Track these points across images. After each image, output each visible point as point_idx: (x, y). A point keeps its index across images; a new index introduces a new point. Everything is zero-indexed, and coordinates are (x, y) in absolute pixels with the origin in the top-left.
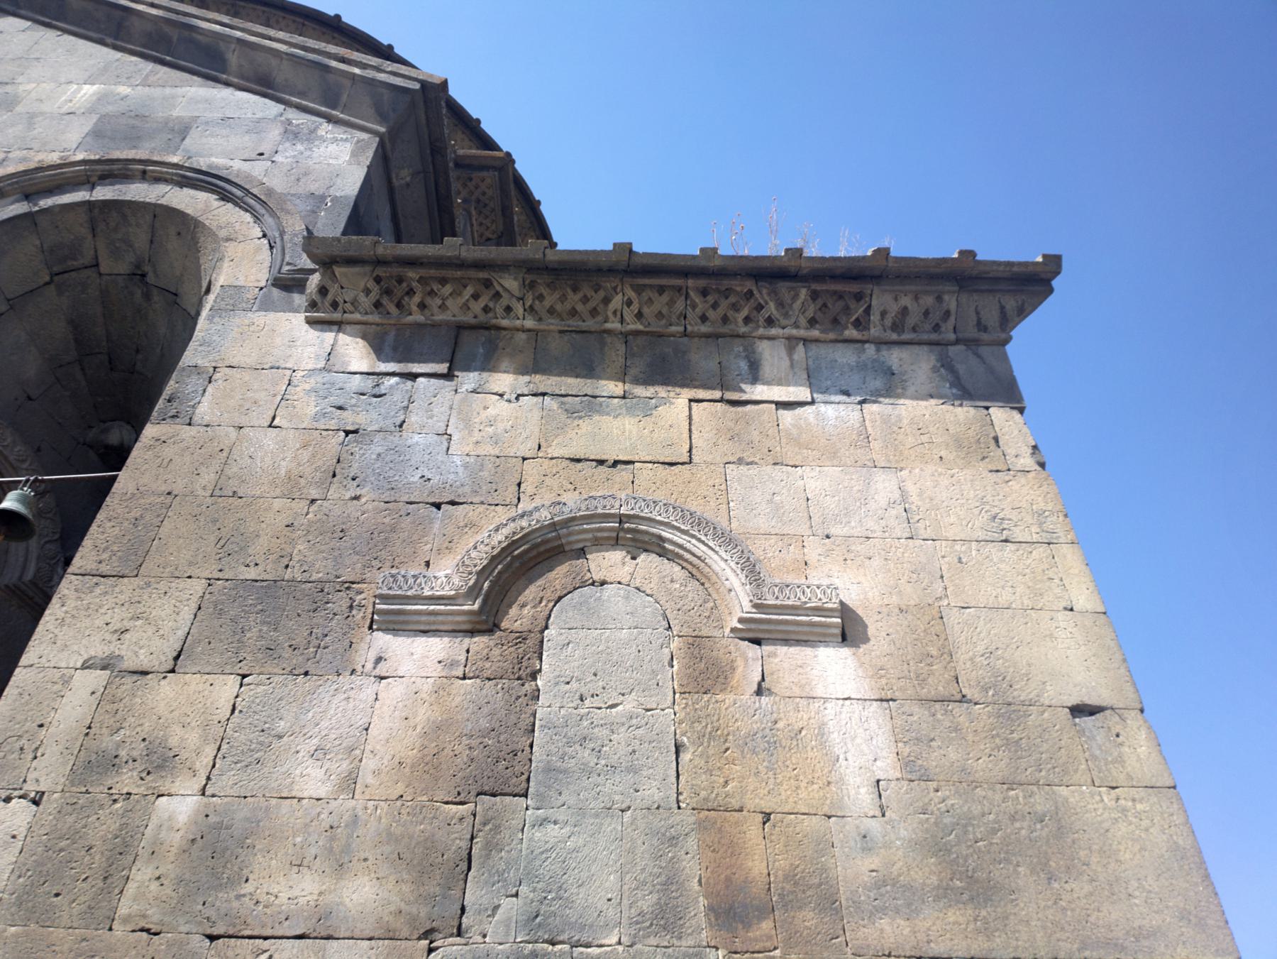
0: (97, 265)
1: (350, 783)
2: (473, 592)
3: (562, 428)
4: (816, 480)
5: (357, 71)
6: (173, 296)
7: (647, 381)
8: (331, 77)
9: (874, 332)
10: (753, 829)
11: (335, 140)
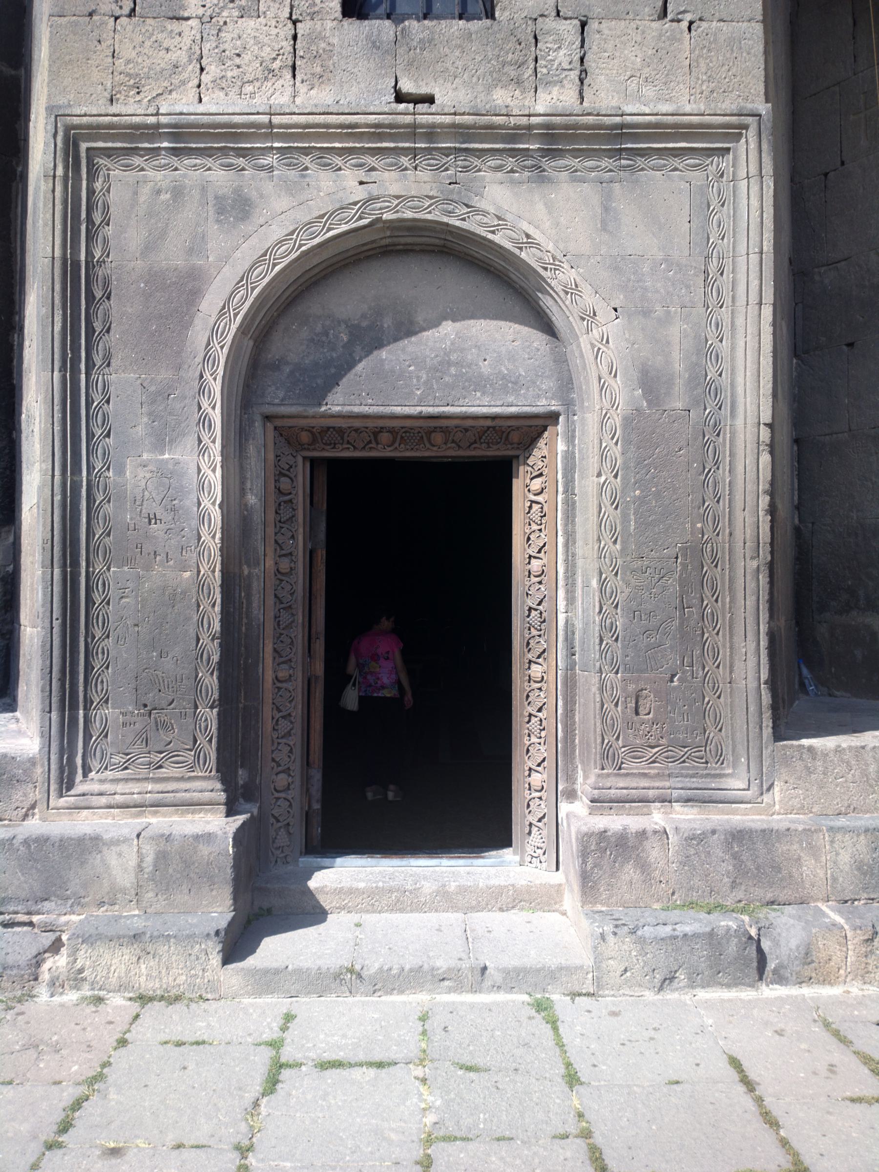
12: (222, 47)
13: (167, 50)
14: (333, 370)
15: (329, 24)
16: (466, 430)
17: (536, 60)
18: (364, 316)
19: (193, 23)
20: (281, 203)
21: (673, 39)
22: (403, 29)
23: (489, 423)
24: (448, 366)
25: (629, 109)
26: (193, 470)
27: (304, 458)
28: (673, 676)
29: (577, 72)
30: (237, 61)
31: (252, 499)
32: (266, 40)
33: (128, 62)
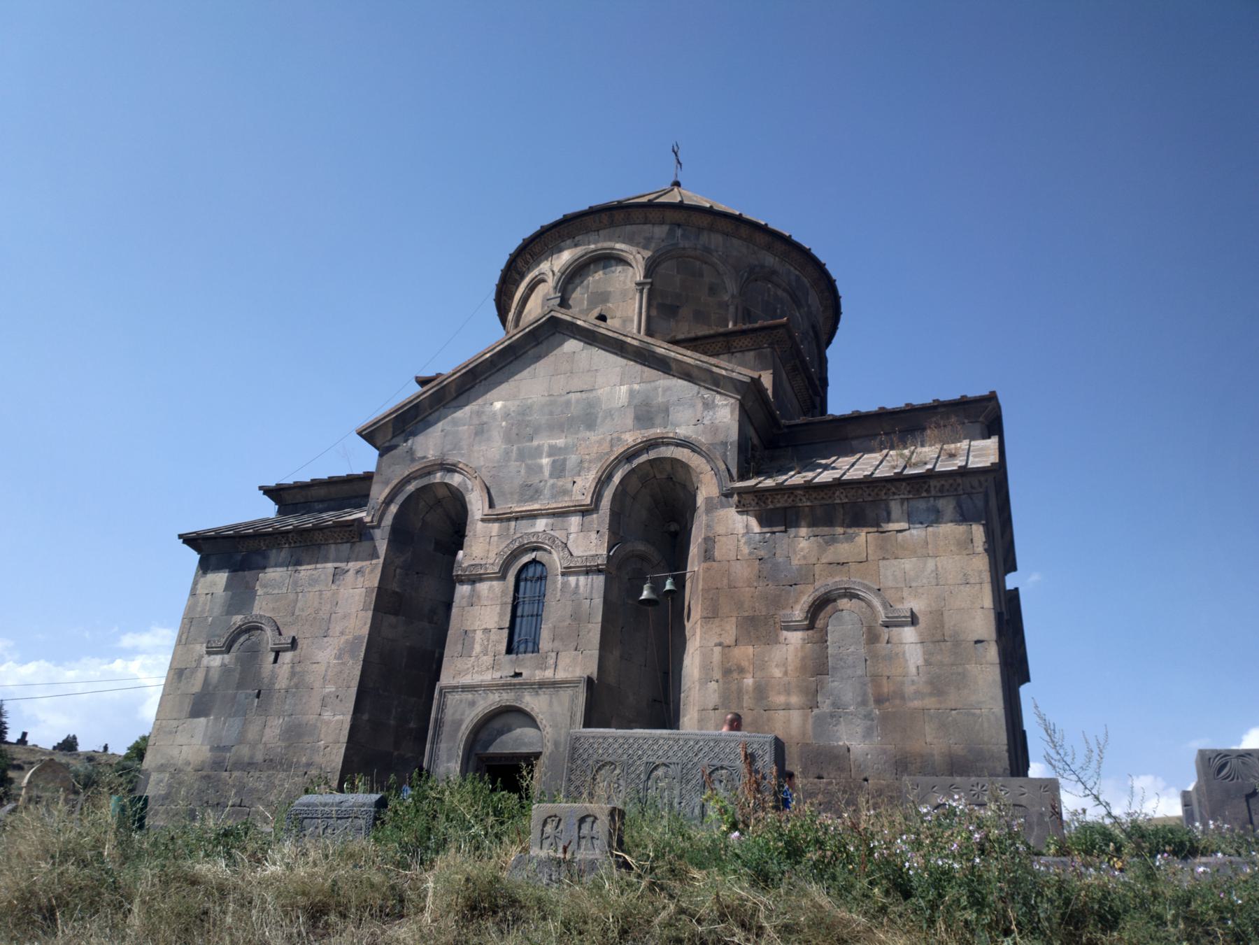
1: (786, 673)
2: (806, 618)
3: (825, 551)
4: (908, 564)
5: (724, 372)
6: (684, 486)
7: (850, 526)
9: (933, 493)
10: (885, 681)
24: (518, 740)
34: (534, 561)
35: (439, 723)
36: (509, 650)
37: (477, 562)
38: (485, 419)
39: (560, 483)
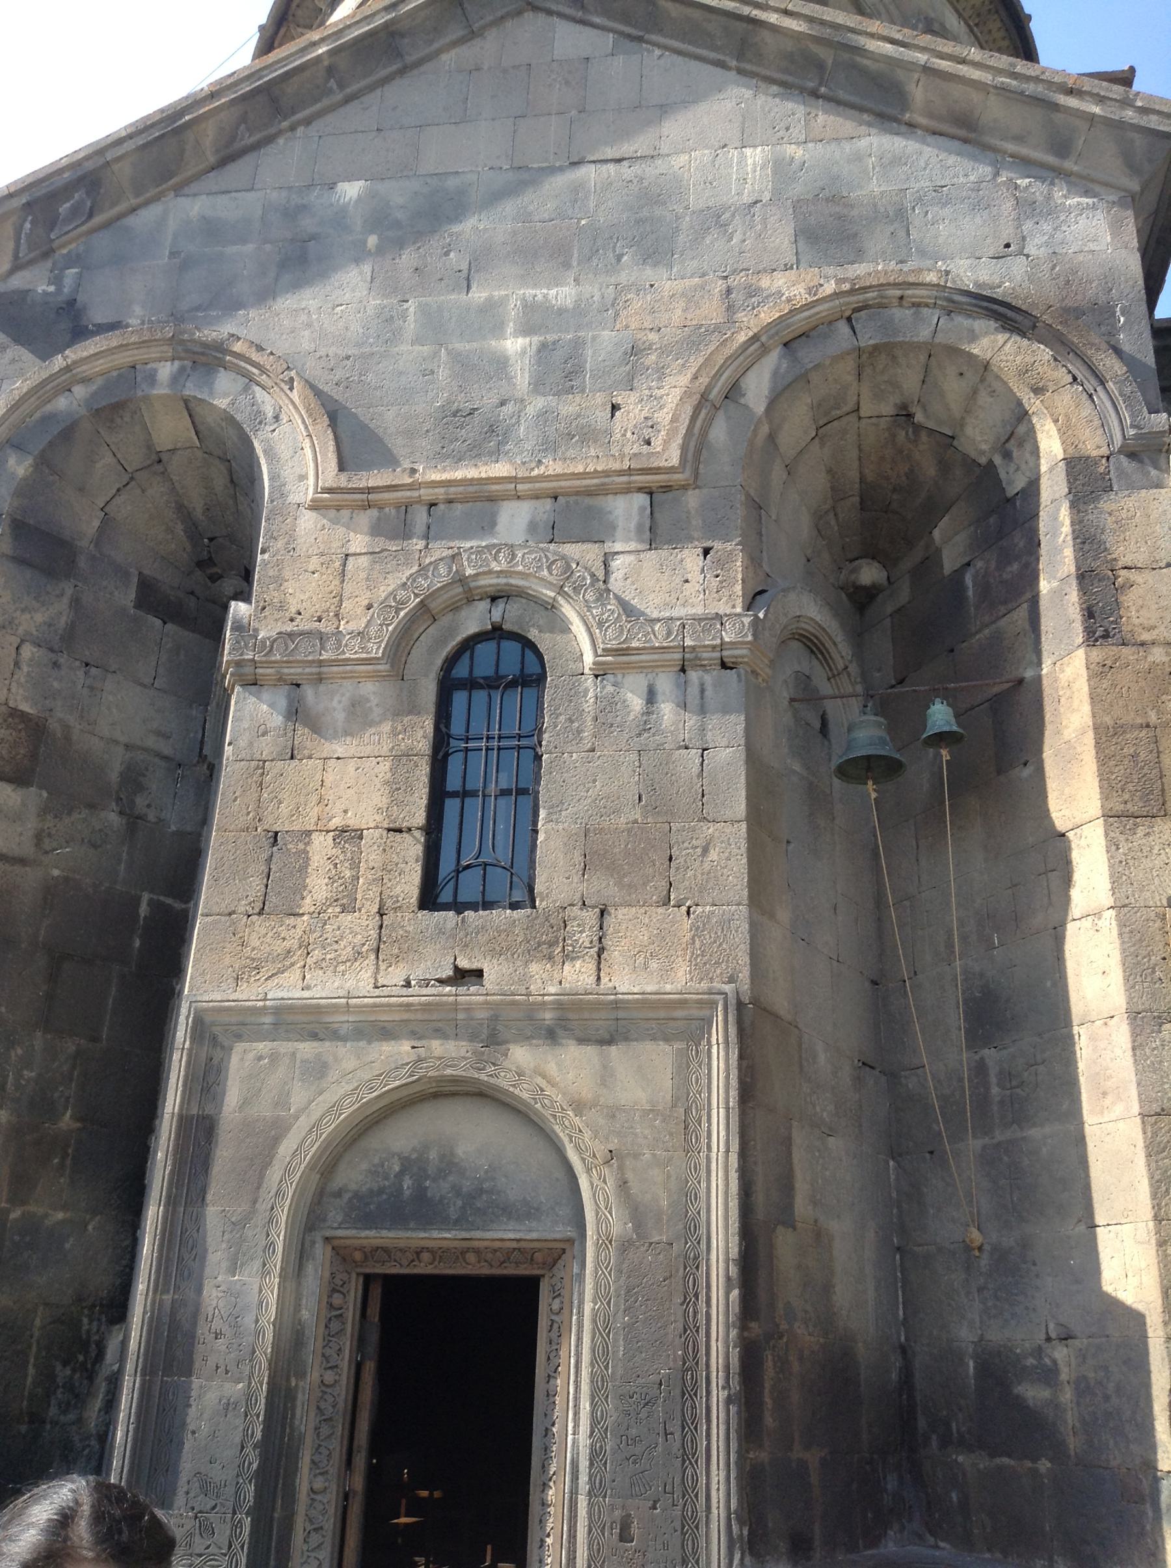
0: (858, 410)
8: (1058, 117)
11: (1082, 209)
12: (325, 936)
13: (284, 939)
14: (384, 1197)
15: (408, 916)
16: (495, 1251)
17: (564, 940)
18: (414, 1149)
19: (305, 918)
20: (350, 1064)
21: (673, 923)
22: (463, 918)
23: (514, 1245)
25: (621, 989)
26: (256, 1290)
27: (358, 1274)
28: (655, 1502)
29: (596, 949)
30: (336, 947)
31: (305, 1314)
32: (358, 930)
33: (253, 949)
34: (497, 633)
35: (200, 1132)
36: (429, 900)
37: (303, 624)
38: (308, 224)
39: (568, 407)
